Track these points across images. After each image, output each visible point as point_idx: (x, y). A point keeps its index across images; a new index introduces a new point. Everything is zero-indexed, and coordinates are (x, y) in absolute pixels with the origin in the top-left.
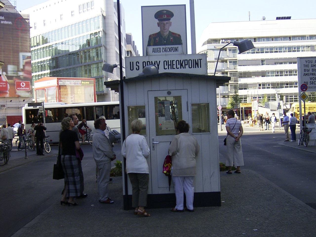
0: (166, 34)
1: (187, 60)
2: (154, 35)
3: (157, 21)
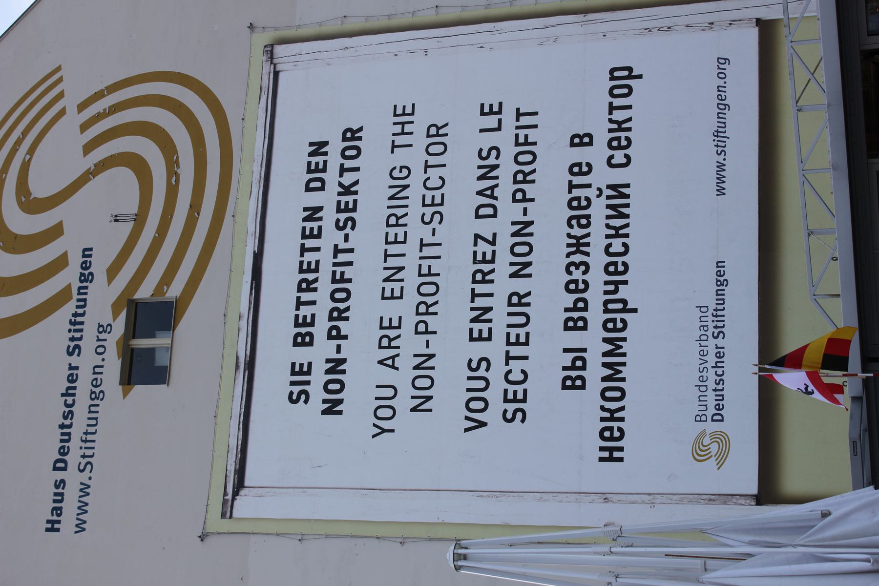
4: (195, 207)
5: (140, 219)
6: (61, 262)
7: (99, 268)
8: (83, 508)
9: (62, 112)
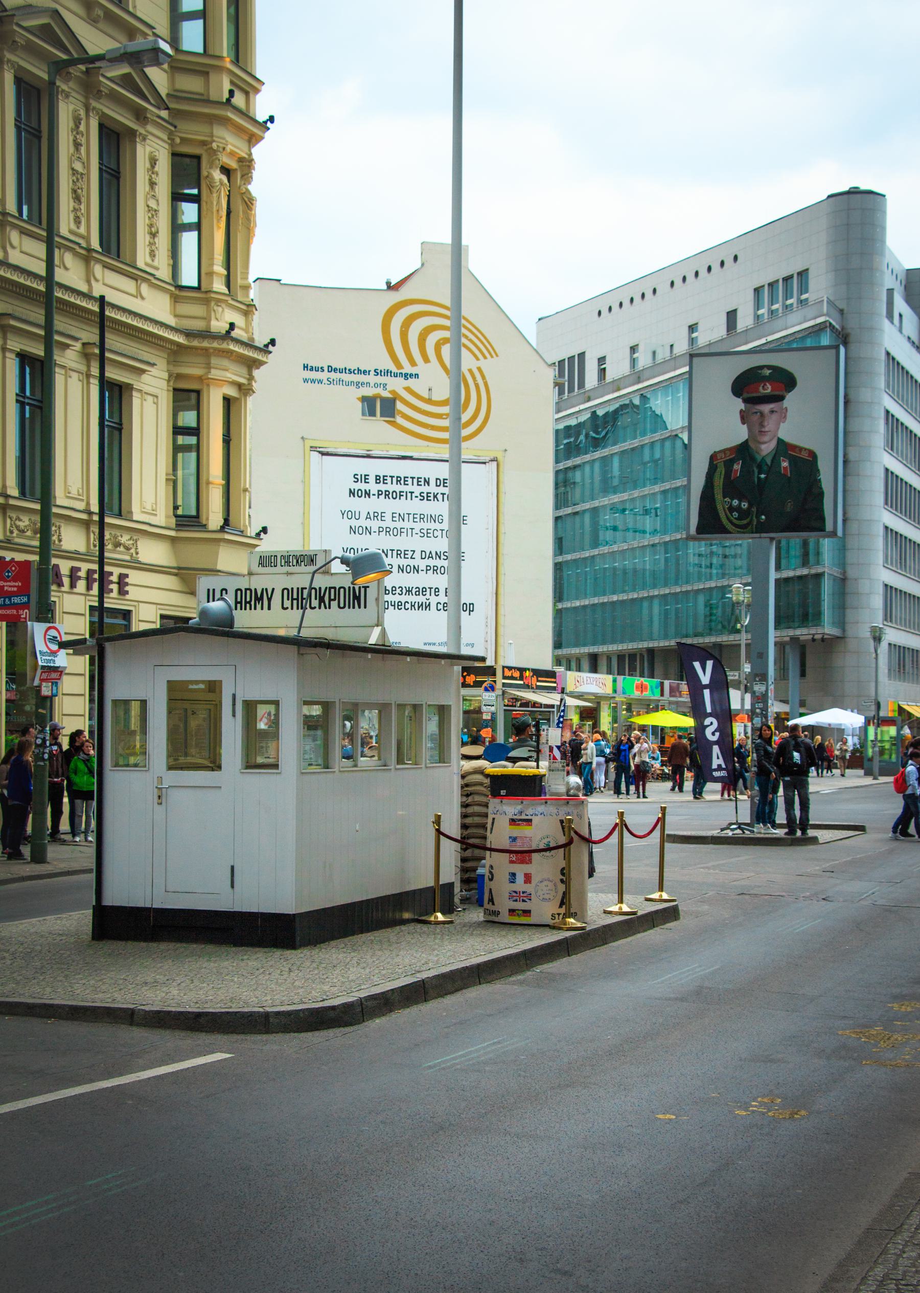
0: (767, 448)
1: (335, 588)
2: (728, 453)
3: (739, 404)
4: (433, 428)
5: (429, 401)
6: (413, 363)
7: (411, 382)
8: (313, 381)
9: (478, 359)
